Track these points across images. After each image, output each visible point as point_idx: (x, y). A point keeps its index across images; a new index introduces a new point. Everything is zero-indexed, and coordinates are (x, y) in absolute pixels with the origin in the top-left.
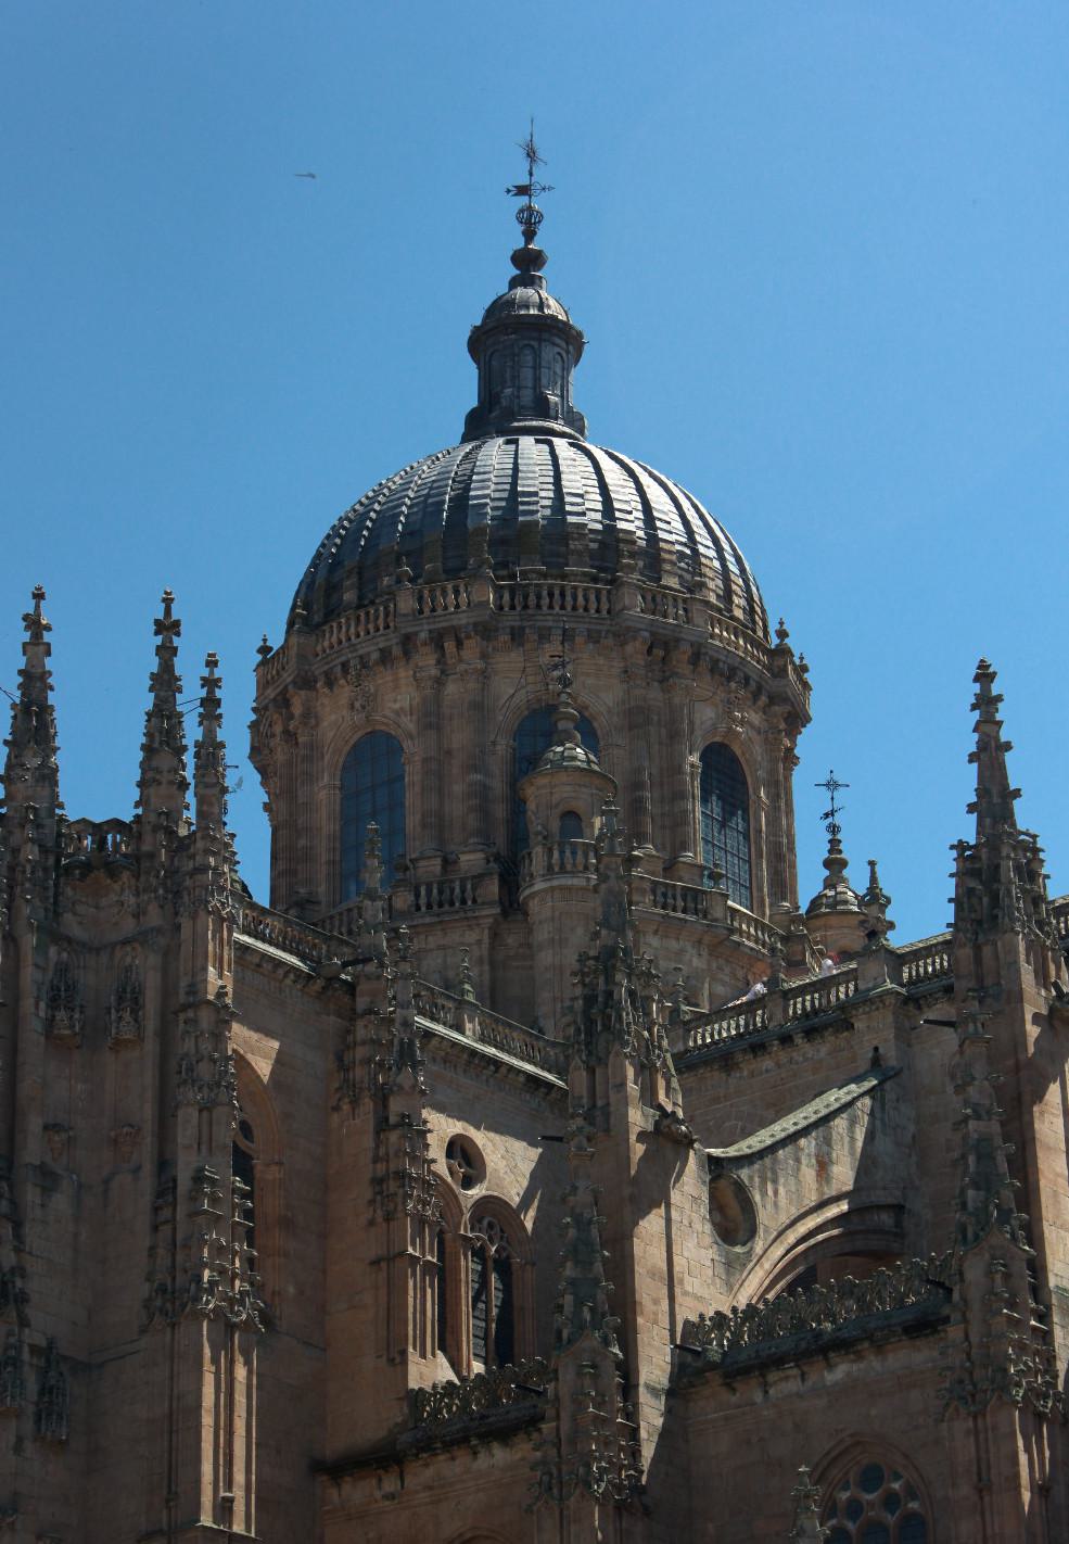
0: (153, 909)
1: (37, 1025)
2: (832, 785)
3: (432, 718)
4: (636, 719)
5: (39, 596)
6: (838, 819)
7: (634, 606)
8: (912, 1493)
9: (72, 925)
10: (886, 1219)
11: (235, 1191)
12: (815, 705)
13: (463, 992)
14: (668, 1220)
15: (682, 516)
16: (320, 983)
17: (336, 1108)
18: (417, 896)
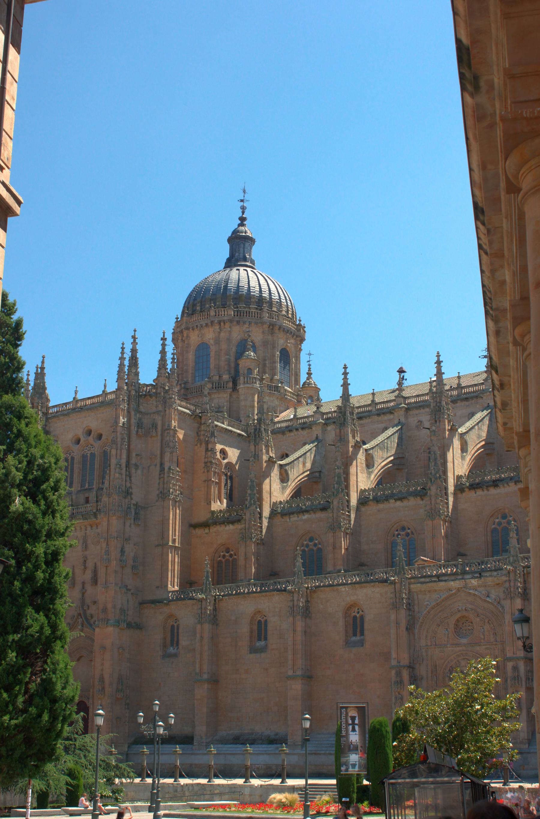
0: (160, 406)
1: (135, 432)
2: (310, 354)
3: (217, 341)
4: (265, 343)
5: (135, 331)
6: (311, 363)
7: (266, 315)
8: (320, 544)
9: (142, 409)
10: (317, 474)
11: (178, 471)
12: (307, 336)
13: (224, 415)
14: (270, 480)
15: (279, 293)
16: (194, 416)
17: (196, 445)
18: (213, 385)
